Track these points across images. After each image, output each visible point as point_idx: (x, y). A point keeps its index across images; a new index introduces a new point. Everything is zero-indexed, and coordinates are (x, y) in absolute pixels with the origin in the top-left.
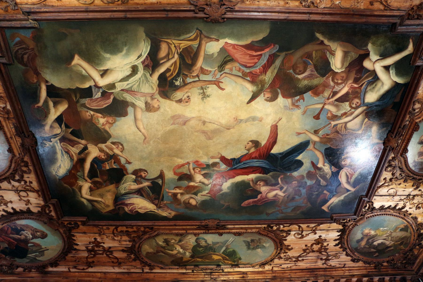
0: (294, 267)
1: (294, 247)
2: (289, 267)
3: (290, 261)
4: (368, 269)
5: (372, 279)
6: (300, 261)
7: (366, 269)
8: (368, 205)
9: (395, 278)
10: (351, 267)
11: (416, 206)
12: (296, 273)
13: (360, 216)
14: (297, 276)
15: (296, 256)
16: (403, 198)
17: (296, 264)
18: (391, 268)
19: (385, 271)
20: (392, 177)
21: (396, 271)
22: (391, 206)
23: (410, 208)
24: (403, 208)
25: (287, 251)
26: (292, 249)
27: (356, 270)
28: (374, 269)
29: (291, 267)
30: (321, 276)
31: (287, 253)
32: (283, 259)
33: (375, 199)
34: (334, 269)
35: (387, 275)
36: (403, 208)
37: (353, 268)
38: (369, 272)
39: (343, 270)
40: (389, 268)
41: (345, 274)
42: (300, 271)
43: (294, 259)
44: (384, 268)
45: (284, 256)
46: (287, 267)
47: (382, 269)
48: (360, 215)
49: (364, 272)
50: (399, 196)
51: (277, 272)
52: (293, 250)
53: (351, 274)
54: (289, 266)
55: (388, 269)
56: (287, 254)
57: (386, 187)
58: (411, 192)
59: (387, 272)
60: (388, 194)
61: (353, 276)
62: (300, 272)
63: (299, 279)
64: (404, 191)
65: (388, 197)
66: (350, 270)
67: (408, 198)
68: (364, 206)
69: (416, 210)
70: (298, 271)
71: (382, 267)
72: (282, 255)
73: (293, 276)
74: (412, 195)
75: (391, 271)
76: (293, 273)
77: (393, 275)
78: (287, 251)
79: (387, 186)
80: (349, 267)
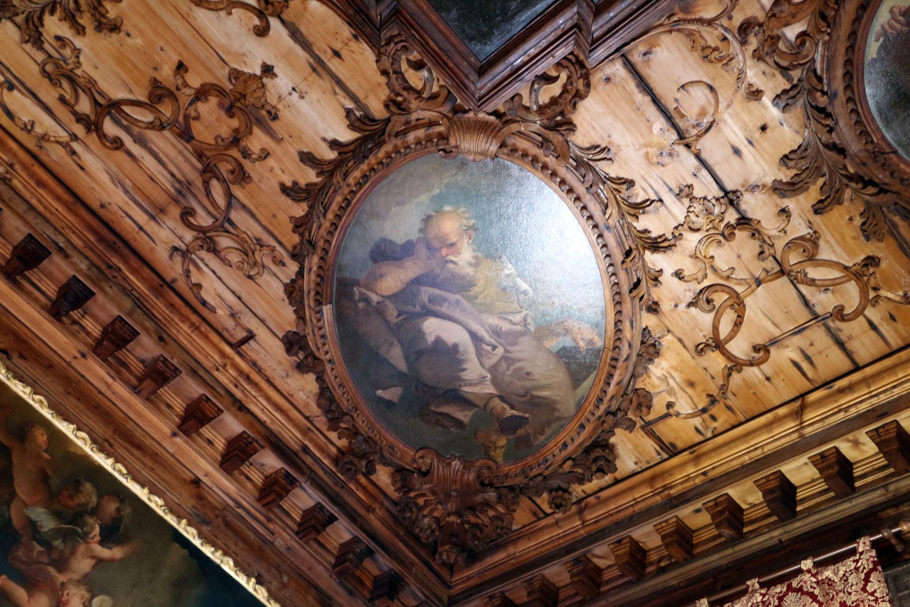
0: (55, 154)
1: (127, 26)
2: (38, 130)
3: (62, 99)
4: (311, 440)
5: (293, 482)
6: (102, 136)
7: (305, 432)
8: (564, 76)
9: (370, 553)
10: (260, 371)
11: (706, 283)
12: (40, 183)
13: (490, 114)
14: (34, 202)
15: (101, 93)
16: (705, 187)
17: (75, 146)
18: (387, 510)
19: (359, 499)
20: (761, 16)
21: (398, 536)
22: (630, 183)
23: (678, 275)
24: (657, 245)
25: (85, 20)
26: (115, 28)
27: (268, 399)
28: (329, 456)
29: (44, 137)
30: (124, 290)
31: (80, 30)
32: (40, 57)
33: (608, 80)
34: (194, 318)
35: (353, 517)
36: (657, 245)
37: (264, 385)
38: (305, 449)
39: (222, 354)
40: (382, 504)
41: (216, 374)
42: (66, 197)
43: (84, 106)
44: (364, 488)
45: (58, 38)
46: (28, 128)
47: (358, 482)
48: (490, 107)
49: (291, 436)
50: (698, 156)
52: (114, 36)
53: (238, 394)
54: (45, 123)
55: (376, 506)
56: (78, 42)
57: (693, 58)
58: (753, 188)
59: (362, 512)
60: (671, 106)
61: (241, 408)
62: (58, 198)
63: (30, 217)
64: (737, 152)
65: (659, 123)
66: (248, 378)
67: (717, 210)
68: (539, 69)
69: (690, 305)
70: (59, 190)
71: (363, 480)
72: (54, 26)
73: (15, 182)
74: (743, 207)
75: (381, 519)
76: (32, 175)
77: (373, 536)
78: (85, 20)
79: (707, 54)
80: (254, 364)
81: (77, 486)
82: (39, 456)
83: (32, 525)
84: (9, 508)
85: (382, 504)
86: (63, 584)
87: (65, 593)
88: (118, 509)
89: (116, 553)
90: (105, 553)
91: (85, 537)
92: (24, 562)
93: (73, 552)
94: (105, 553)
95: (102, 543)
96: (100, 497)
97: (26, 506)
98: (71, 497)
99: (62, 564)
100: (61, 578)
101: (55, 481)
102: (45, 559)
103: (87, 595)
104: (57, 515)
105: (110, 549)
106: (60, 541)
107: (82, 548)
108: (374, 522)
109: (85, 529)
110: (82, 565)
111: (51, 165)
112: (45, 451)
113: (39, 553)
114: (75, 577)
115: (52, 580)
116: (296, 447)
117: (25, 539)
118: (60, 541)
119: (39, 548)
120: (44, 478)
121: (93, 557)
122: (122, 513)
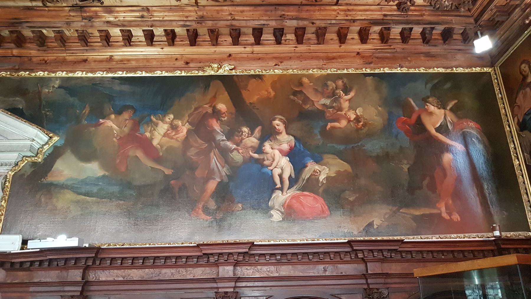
4: (385, 11)
5: (389, 29)
7: (381, 10)
9: (433, 29)
10: (350, 5)
18: (429, 10)
19: (416, 15)
21: (439, 15)
27: (360, 11)
28: (395, 10)
30: (290, 19)
34: (317, 8)
35: (418, 23)
37: (355, 8)
38: (385, 15)
39: (334, 10)
40: (425, 10)
41: (337, 18)
44: (415, 10)
47: (412, 10)
49: (377, 15)
51: (206, 7)
53: (350, 18)
55: (424, 12)
59: (420, 18)
61: (354, 21)
66: (349, 10)
71: (412, 8)
75: (429, 15)
77: (430, 23)
80: (347, 4)
81: (326, 85)
82: (310, 85)
83: (324, 105)
84: (314, 105)
85: (425, 10)
86: (345, 114)
87: (348, 115)
88: (343, 82)
89: (352, 94)
90: (349, 97)
91: (340, 97)
92: (331, 116)
93: (340, 103)
94: (349, 97)
95: (346, 95)
96: (335, 82)
97: (318, 102)
98: (327, 90)
99: (340, 109)
100: (343, 113)
101: (320, 89)
102: (335, 111)
103: (354, 112)
104: (328, 97)
105: (349, 94)
106: (335, 103)
107: (342, 100)
108: (427, 18)
109: (338, 95)
110: (346, 105)
111: (239, 3)
112: (310, 83)
113: (332, 111)
114: (347, 110)
115: (341, 115)
116: (382, 17)
117: (326, 110)
118: (335, 103)
119: (331, 110)
120: (316, 90)
121: (347, 101)
122: (344, 82)
